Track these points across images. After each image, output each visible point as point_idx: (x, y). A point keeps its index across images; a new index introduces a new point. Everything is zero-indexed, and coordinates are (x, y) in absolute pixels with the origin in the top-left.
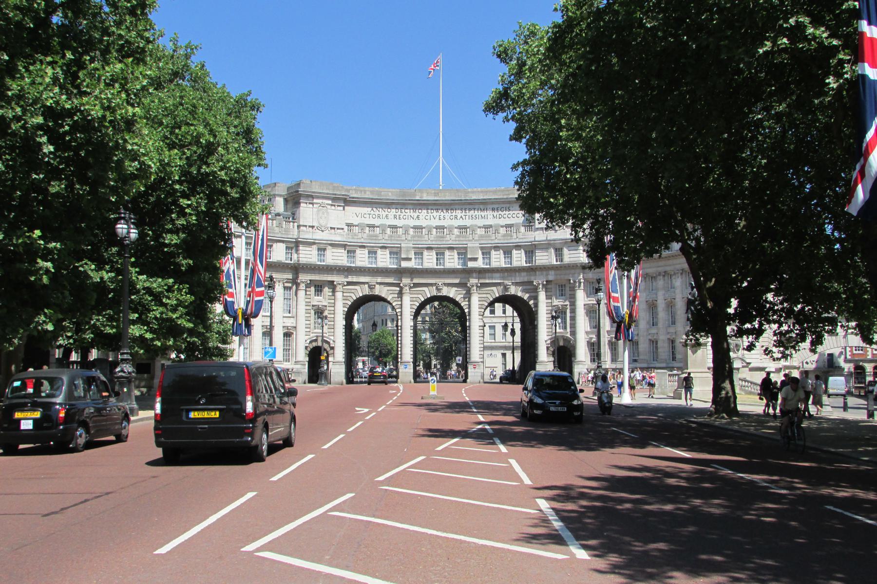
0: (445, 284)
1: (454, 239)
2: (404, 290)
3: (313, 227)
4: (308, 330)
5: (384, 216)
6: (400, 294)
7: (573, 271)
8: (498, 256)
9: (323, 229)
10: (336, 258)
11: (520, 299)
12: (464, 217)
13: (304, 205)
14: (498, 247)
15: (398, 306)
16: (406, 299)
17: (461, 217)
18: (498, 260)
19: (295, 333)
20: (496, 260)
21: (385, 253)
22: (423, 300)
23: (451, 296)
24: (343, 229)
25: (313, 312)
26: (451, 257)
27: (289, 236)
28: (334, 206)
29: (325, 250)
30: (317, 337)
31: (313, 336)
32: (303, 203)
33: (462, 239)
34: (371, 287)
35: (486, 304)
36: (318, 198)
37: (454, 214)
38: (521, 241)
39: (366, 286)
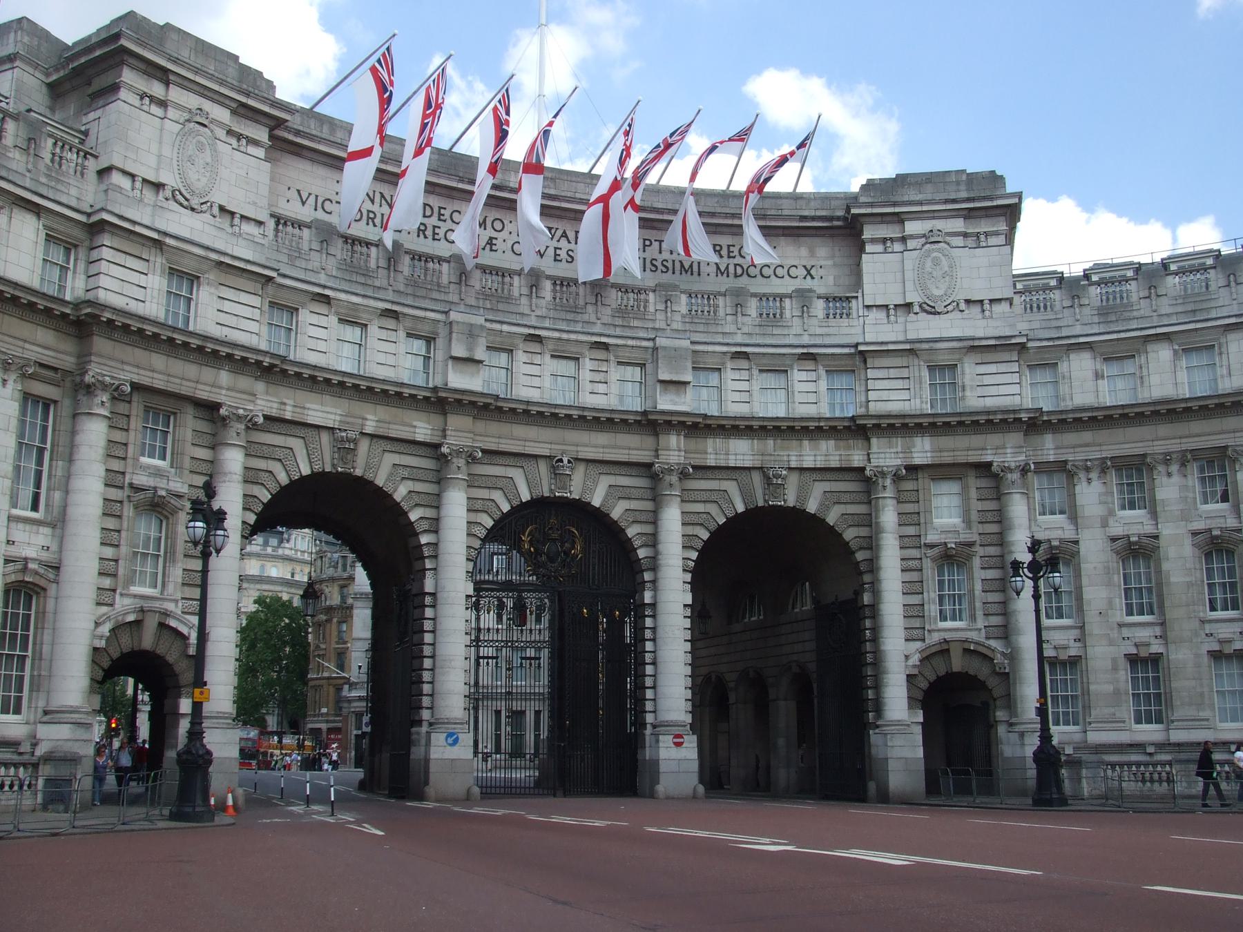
0: (577, 459)
1: (606, 319)
2: (454, 467)
3: (158, 186)
4: (107, 582)
6: (440, 480)
7: (994, 439)
8: (744, 386)
9: (195, 202)
11: (816, 522)
14: (745, 356)
15: (424, 525)
16: (456, 504)
18: (745, 397)
19: (52, 590)
20: (737, 397)
21: (392, 336)
22: (506, 507)
23: (596, 502)
24: (260, 223)
26: (598, 377)
27: (64, 199)
28: (239, 137)
29: (193, 279)
30: (142, 610)
31: (124, 606)
32: (131, 88)
33: (636, 323)
34: (345, 448)
35: (705, 535)
36: (187, 85)
38: (819, 341)
39: (325, 437)
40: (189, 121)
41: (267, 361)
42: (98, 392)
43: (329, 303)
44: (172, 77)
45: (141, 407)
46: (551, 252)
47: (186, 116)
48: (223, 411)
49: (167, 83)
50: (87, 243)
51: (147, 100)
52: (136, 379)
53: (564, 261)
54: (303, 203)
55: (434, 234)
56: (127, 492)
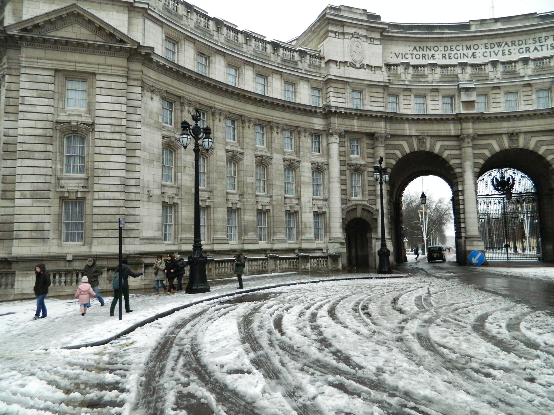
0: (520, 132)
3: (346, 62)
5: (430, 57)
10: (376, 104)
12: (539, 48)
13: (333, 35)
17: (536, 49)
25: (348, 173)
32: (332, 32)
37: (524, 46)
39: (414, 139)
40: (353, 37)
41: (389, 115)
42: (334, 135)
43: (410, 91)
44: (345, 24)
45: (349, 139)
46: (501, 53)
47: (351, 36)
48: (376, 135)
49: (343, 26)
50: (325, 88)
51: (337, 34)
52: (345, 129)
53: (507, 55)
54: (397, 57)
55: (449, 57)
56: (347, 166)
